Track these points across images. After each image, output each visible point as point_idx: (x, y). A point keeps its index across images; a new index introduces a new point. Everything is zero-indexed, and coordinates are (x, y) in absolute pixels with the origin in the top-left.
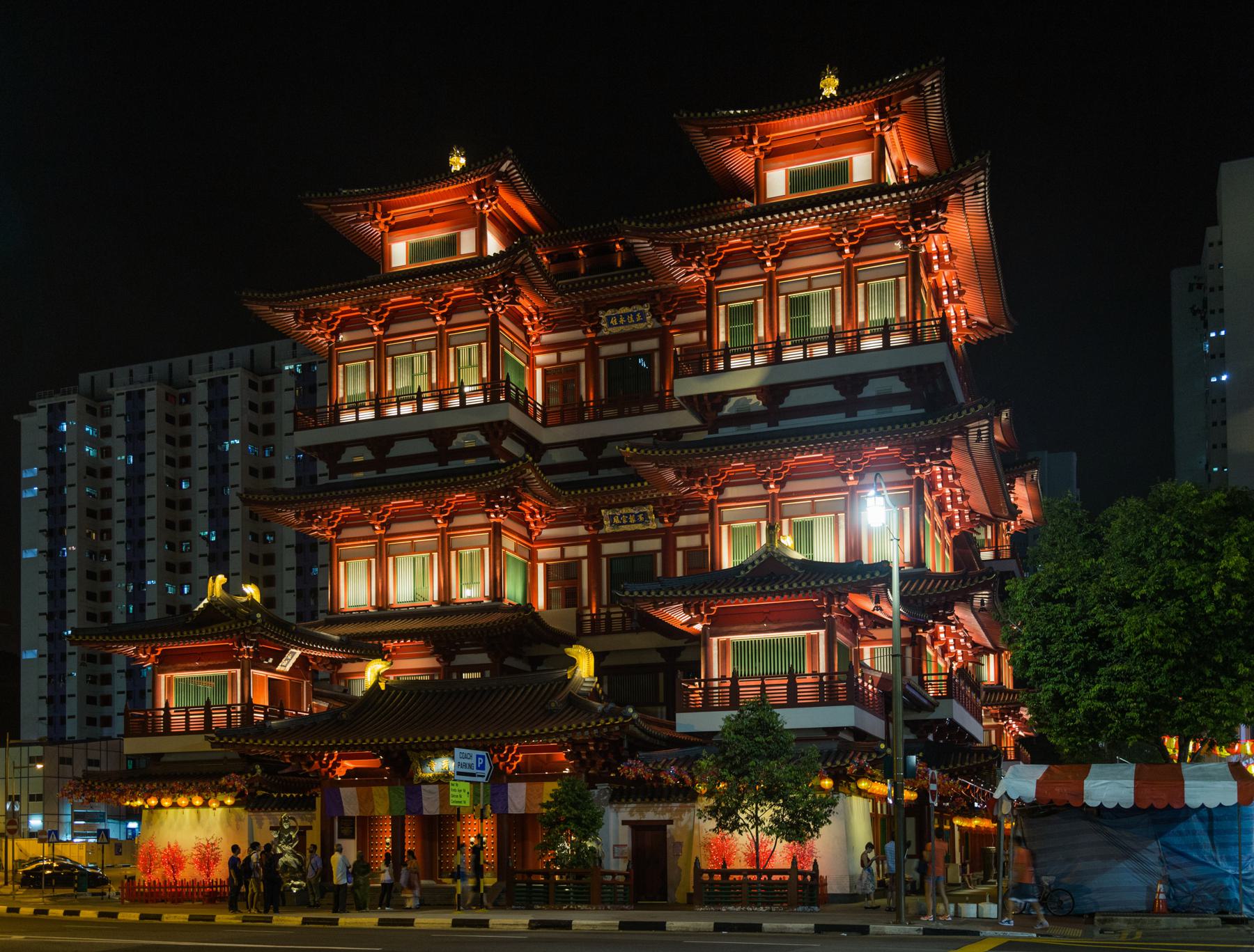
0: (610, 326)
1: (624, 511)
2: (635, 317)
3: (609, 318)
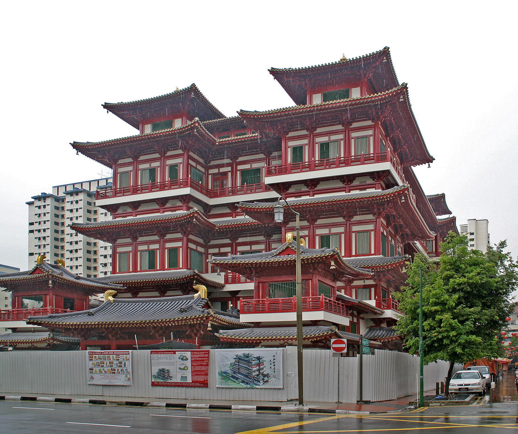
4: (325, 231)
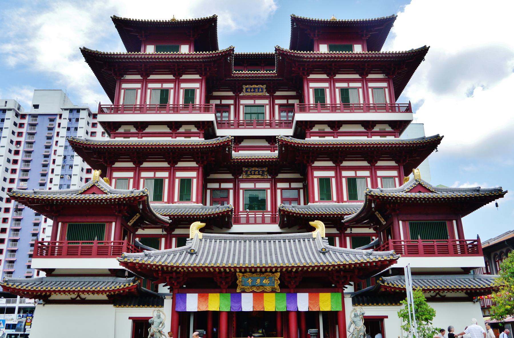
0: (247, 92)
1: (253, 169)
2: (258, 90)
3: (247, 89)
4: (351, 174)
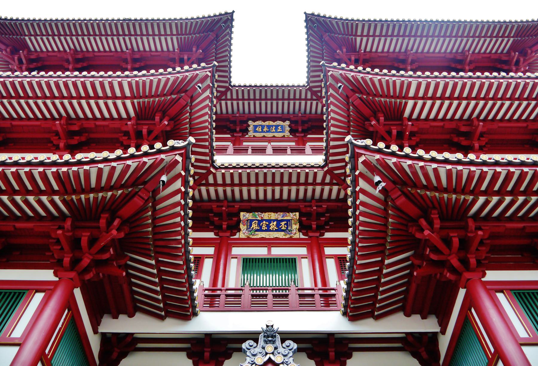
0: (255, 131)
3: (255, 127)
